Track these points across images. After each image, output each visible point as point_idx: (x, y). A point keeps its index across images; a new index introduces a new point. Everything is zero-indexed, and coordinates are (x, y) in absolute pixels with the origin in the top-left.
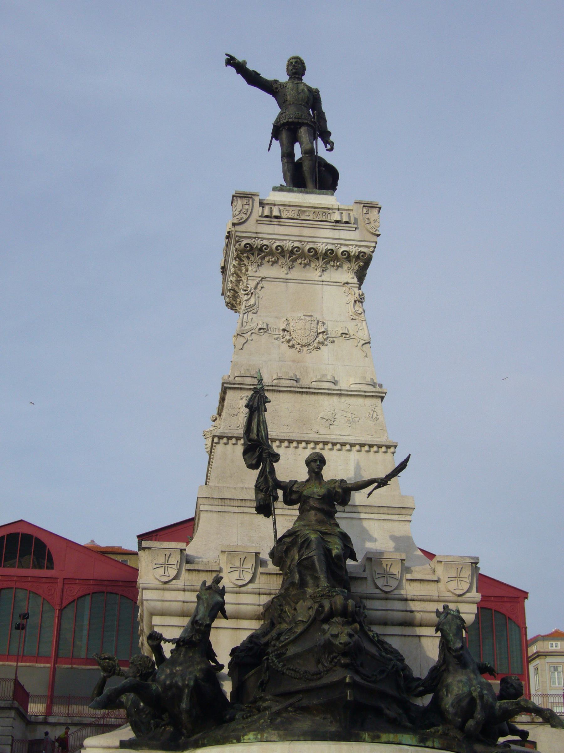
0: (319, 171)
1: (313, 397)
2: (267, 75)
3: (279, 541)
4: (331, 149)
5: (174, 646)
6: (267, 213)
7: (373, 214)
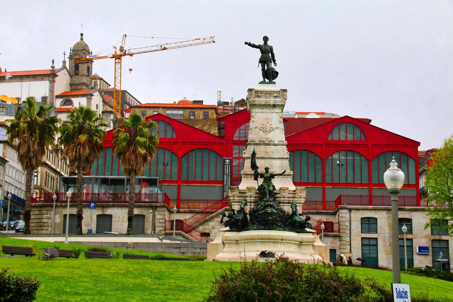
0: (272, 74)
1: (269, 146)
2: (257, 44)
3: (259, 187)
4: (276, 65)
5: (237, 212)
6: (257, 95)
7: (285, 93)
